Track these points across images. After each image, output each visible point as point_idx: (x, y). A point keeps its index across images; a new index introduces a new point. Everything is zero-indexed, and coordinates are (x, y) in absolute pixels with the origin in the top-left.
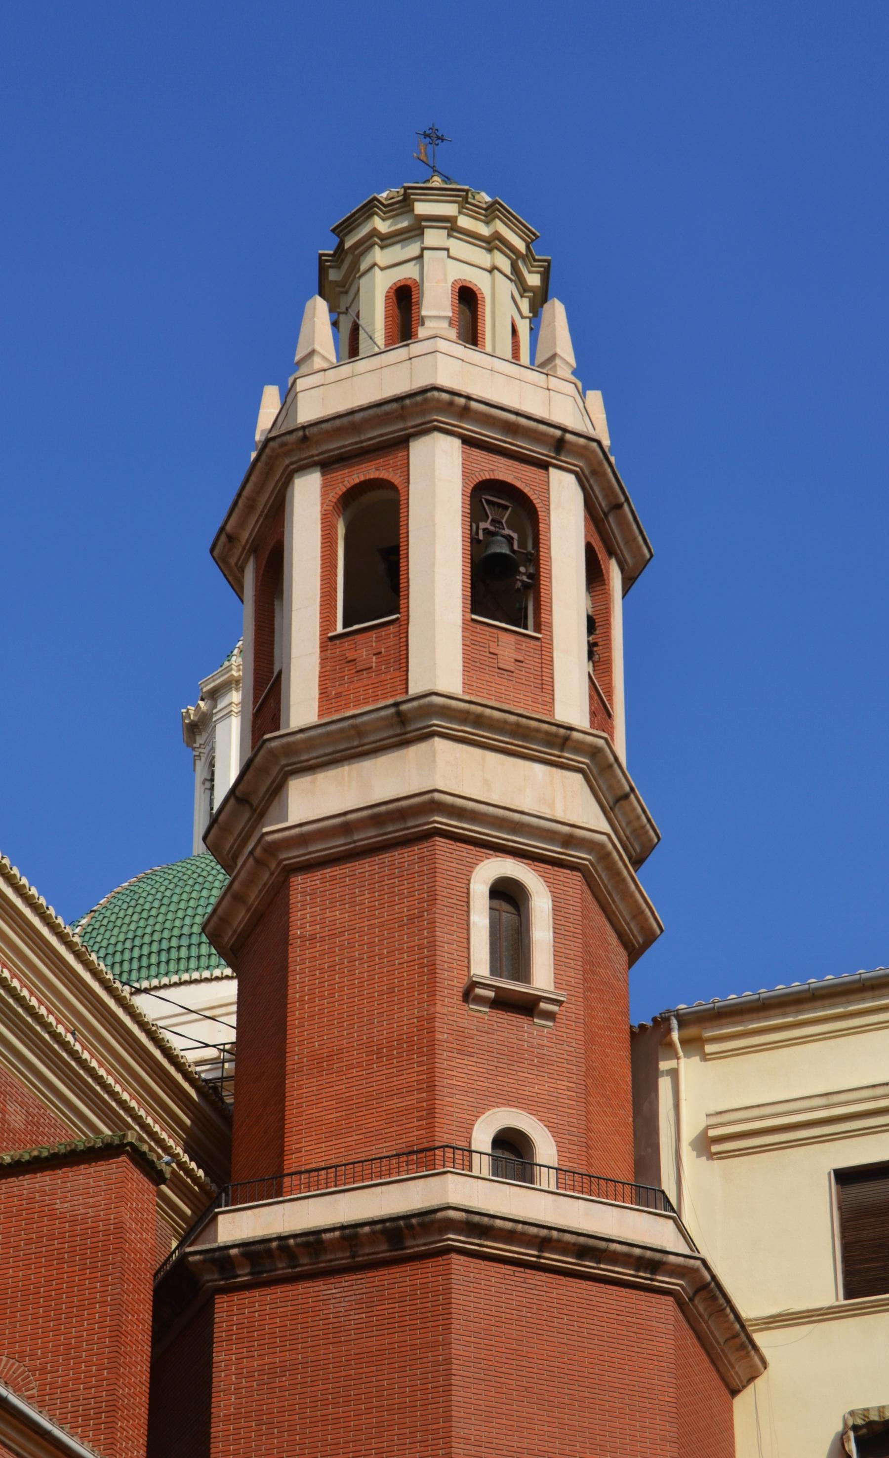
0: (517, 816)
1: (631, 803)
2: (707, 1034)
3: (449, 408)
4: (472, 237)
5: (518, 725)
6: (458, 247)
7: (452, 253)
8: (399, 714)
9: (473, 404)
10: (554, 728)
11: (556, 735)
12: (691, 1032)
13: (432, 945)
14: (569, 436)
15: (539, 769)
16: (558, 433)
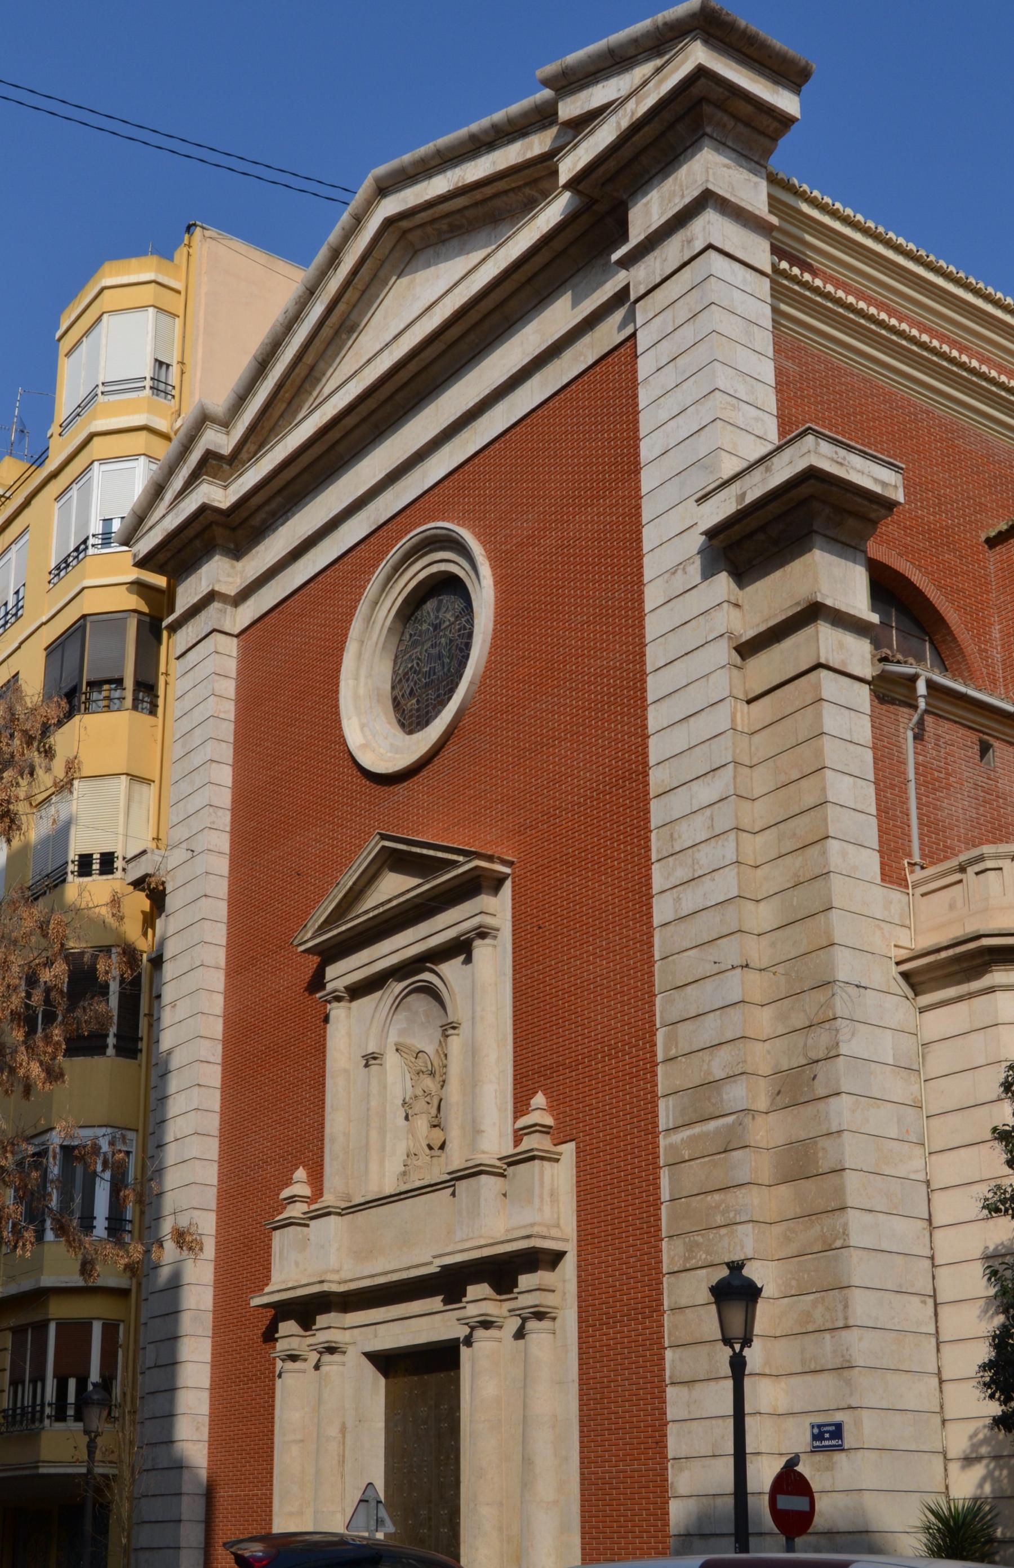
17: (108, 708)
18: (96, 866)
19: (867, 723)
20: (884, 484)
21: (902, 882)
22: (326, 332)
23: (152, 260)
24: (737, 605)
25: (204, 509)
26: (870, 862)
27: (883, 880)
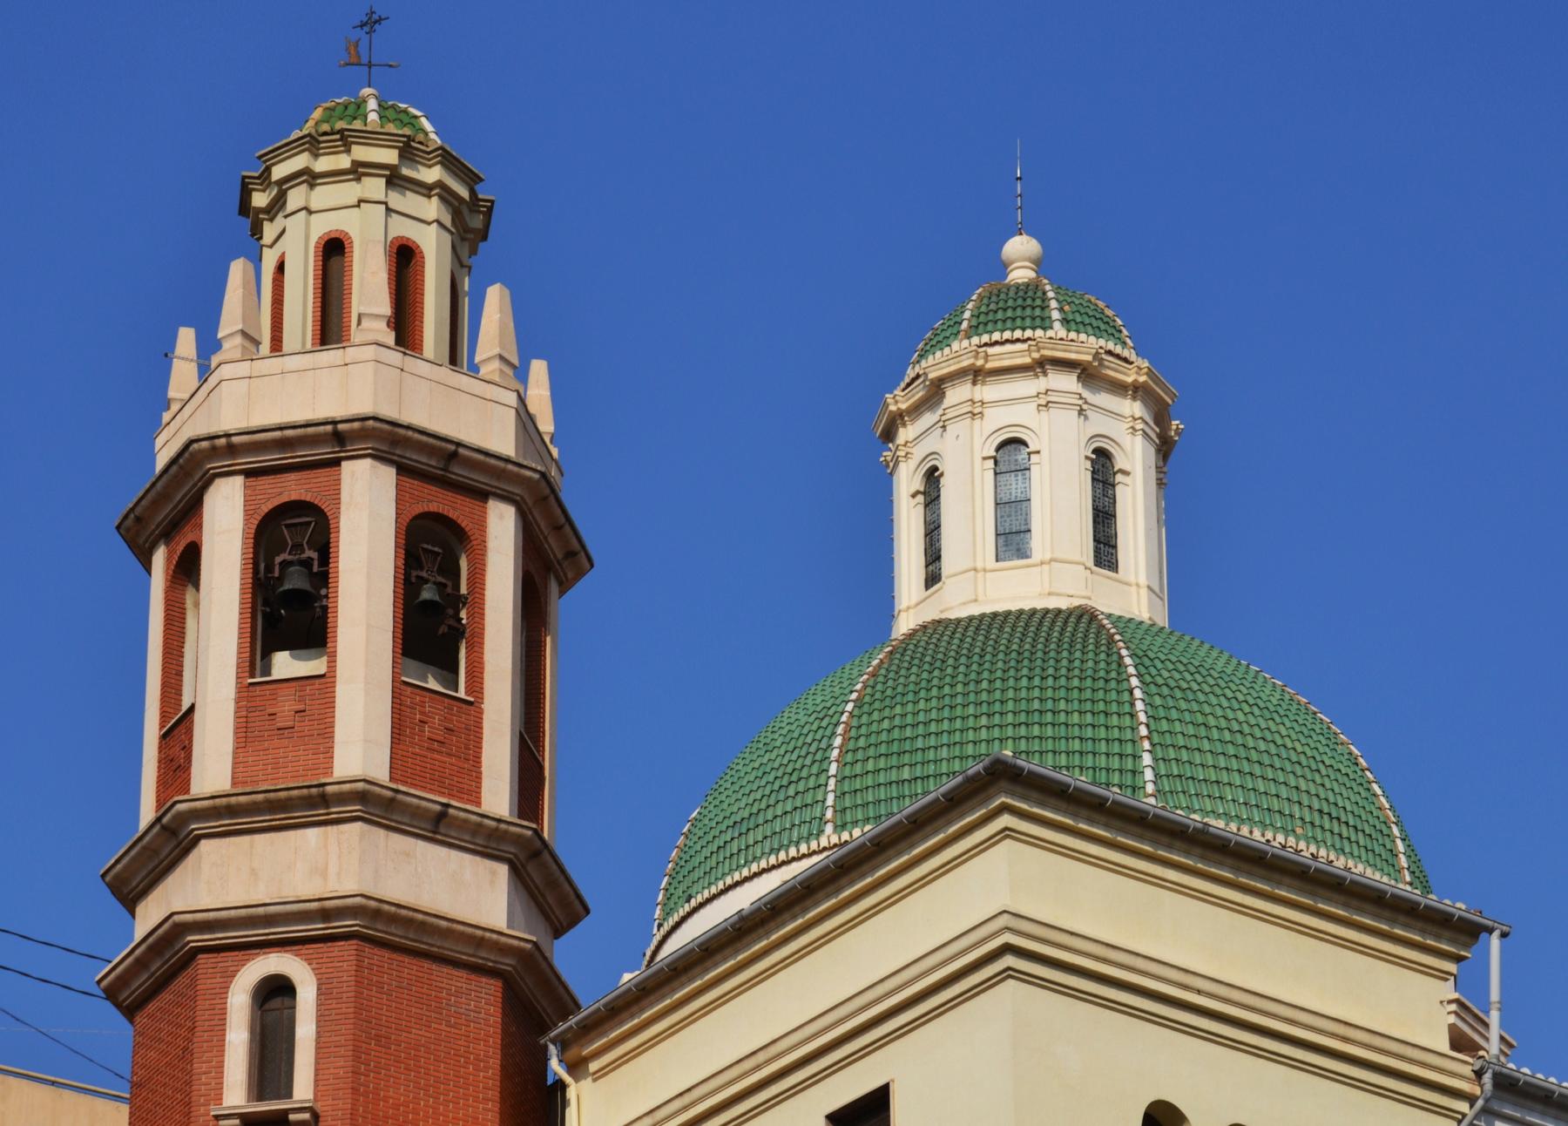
0: (261, 910)
1: (456, 818)
3: (214, 452)
4: (335, 175)
5: (268, 801)
6: (323, 196)
7: (313, 207)
8: (164, 828)
9: (235, 439)
10: (305, 791)
11: (310, 797)
13: (189, 1083)
14: (341, 427)
16: (329, 428)
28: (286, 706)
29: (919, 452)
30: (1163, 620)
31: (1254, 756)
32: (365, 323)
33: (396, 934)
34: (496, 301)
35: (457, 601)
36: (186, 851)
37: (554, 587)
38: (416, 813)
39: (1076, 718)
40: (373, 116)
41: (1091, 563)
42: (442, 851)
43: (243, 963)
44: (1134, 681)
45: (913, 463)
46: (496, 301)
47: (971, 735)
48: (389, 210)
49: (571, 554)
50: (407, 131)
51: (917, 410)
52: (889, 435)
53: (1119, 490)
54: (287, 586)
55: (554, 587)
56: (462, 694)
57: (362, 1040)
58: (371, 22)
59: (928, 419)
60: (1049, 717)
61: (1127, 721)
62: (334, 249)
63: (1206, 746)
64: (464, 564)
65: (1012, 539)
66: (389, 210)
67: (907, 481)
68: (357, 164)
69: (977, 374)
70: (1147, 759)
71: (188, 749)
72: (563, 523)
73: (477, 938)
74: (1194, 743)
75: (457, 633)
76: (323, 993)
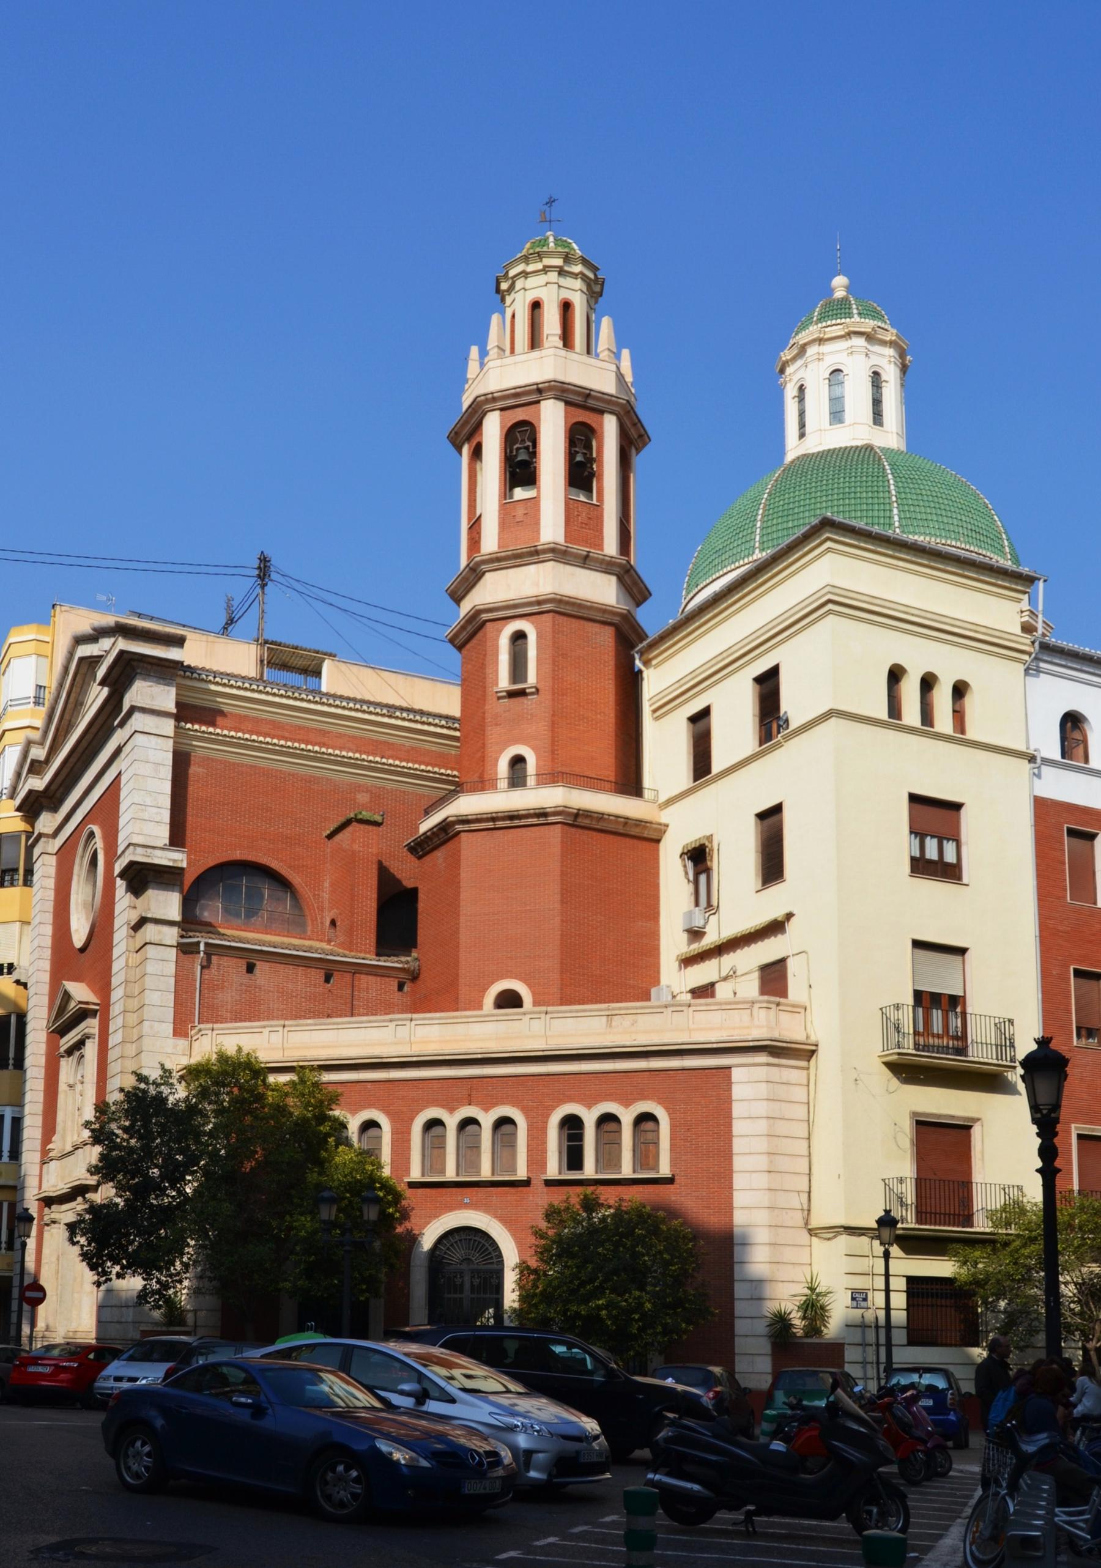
2: (651, 656)
12: (645, 657)
15: (532, 567)
17: (12, 885)
18: (5, 971)
19: (173, 966)
20: (175, 861)
21: (185, 1035)
22: (70, 706)
23: (33, 627)
24: (135, 908)
25: (30, 792)
26: (169, 1028)
27: (174, 1035)
28: (520, 511)
29: (795, 378)
30: (903, 448)
31: (943, 507)
32: (550, 338)
33: (568, 610)
34: (606, 324)
35: (591, 460)
36: (480, 578)
37: (633, 451)
38: (576, 556)
39: (864, 495)
40: (552, 245)
41: (871, 423)
42: (588, 572)
43: (505, 625)
44: (890, 476)
45: (793, 383)
46: (606, 324)
47: (818, 505)
48: (559, 286)
49: (641, 436)
50: (566, 250)
51: (794, 359)
52: (782, 371)
53: (884, 390)
54: (519, 459)
55: (633, 451)
56: (594, 502)
57: (557, 656)
58: (551, 202)
59: (799, 363)
60: (852, 495)
61: (887, 494)
62: (536, 305)
63: (921, 503)
64: (594, 443)
65: (837, 415)
66: (559, 286)
67: (790, 391)
68: (545, 267)
69: (821, 341)
70: (895, 511)
71: (479, 533)
72: (637, 423)
73: (604, 610)
74: (916, 503)
75: (592, 475)
76: (540, 636)
